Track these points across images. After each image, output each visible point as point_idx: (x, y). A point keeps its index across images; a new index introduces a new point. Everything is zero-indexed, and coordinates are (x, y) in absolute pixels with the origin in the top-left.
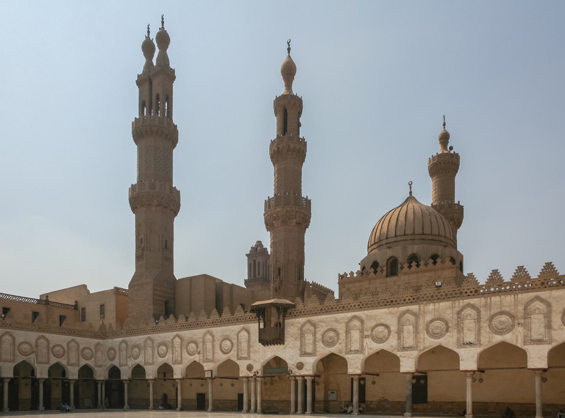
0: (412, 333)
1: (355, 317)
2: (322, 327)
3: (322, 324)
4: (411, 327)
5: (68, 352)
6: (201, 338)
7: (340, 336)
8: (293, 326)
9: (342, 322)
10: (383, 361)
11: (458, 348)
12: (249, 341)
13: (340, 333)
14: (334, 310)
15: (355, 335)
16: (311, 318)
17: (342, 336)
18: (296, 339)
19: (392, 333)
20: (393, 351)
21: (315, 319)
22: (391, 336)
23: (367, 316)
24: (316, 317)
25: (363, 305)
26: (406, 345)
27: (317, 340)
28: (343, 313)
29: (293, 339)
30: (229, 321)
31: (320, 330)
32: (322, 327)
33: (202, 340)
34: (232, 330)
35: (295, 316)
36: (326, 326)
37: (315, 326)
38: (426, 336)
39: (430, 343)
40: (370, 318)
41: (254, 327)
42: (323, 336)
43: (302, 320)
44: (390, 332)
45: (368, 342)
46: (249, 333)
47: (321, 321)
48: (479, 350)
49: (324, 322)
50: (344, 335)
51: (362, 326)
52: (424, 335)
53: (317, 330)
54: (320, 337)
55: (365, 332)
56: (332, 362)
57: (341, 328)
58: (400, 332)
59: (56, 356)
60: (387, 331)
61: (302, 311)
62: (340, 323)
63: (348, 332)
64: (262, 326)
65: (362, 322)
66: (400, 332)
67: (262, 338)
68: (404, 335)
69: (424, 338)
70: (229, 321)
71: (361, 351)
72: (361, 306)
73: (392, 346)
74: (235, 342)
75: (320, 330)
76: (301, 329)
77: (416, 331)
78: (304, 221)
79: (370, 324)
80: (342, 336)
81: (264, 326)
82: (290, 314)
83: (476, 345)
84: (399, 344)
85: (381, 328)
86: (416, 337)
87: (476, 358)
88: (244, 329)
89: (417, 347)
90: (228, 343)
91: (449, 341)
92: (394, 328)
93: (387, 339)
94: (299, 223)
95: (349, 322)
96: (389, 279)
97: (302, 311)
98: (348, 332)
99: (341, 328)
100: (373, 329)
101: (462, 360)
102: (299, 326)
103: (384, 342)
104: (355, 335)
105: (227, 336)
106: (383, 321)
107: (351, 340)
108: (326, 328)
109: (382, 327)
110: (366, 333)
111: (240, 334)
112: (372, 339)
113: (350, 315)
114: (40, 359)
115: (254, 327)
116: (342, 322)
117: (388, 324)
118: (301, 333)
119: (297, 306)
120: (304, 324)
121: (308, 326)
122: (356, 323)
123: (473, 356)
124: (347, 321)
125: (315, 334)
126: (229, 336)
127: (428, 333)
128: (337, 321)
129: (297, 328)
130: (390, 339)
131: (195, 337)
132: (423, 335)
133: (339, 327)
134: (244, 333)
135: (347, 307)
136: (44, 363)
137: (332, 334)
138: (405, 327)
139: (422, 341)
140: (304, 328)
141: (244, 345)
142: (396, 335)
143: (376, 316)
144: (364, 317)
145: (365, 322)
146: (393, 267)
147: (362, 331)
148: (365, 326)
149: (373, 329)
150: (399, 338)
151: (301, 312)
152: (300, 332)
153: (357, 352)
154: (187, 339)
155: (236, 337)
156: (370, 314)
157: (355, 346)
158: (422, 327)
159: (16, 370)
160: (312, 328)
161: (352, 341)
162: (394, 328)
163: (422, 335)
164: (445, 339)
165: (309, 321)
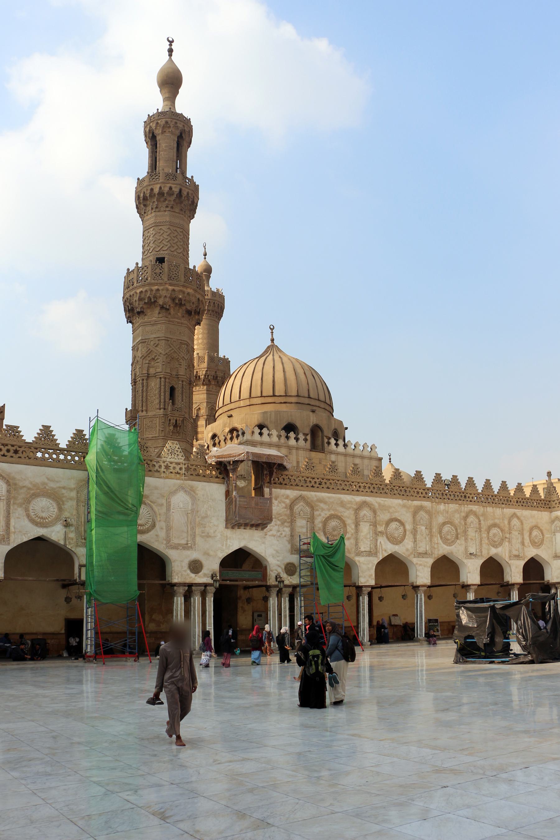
2: (323, 510)
6: (71, 490)
7: (348, 527)
9: (350, 508)
15: (365, 528)
18: (283, 523)
20: (409, 555)
23: (379, 504)
29: (279, 523)
31: (320, 515)
32: (323, 510)
36: (329, 510)
37: (312, 506)
40: (384, 508)
42: (325, 523)
43: (292, 493)
45: (382, 540)
47: (321, 501)
49: (325, 503)
50: (353, 527)
51: (375, 517)
53: (316, 513)
54: (320, 525)
62: (348, 509)
63: (357, 525)
65: (375, 512)
75: (320, 515)
76: (291, 507)
79: (384, 517)
85: (394, 525)
99: (348, 515)
100: (388, 523)
102: (288, 501)
104: (365, 528)
106: (396, 515)
108: (328, 513)
109: (396, 523)
110: (381, 528)
113: (359, 499)
116: (350, 508)
117: (402, 520)
124: (355, 507)
128: (342, 504)
129: (284, 505)
131: (52, 485)
133: (346, 514)
143: (390, 507)
144: (377, 506)
145: (378, 513)
147: (374, 524)
148: (378, 518)
149: (388, 523)
152: (288, 512)
154: (27, 483)
156: (382, 502)
160: (308, 509)
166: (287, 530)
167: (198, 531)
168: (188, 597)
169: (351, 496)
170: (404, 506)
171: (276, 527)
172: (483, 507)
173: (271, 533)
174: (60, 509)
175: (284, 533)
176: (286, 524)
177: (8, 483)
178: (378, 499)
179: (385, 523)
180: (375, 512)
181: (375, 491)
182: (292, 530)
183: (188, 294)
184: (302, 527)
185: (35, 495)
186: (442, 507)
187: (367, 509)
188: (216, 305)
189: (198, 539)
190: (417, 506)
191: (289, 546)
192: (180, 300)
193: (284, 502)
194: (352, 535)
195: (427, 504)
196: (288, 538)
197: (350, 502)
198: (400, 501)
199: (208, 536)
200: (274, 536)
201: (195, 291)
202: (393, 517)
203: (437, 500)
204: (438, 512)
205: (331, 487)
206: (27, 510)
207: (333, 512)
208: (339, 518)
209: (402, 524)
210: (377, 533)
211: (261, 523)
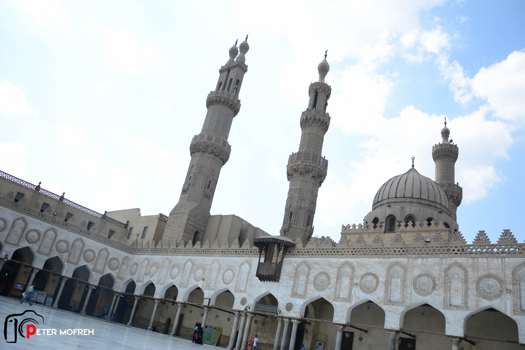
0: (399, 287)
1: (347, 263)
2: (316, 269)
3: (316, 266)
4: (399, 280)
5: (97, 259)
8: (290, 264)
9: (335, 267)
10: (369, 313)
11: (444, 309)
12: (249, 273)
13: (331, 277)
14: (329, 253)
15: (346, 281)
16: (306, 259)
17: (333, 281)
19: (380, 284)
21: (311, 260)
22: (379, 288)
23: (358, 263)
24: (312, 259)
25: (356, 252)
26: (393, 299)
27: (309, 281)
28: (336, 257)
29: (288, 278)
30: (236, 252)
31: (313, 272)
32: (316, 269)
33: (209, 267)
34: (236, 260)
35: (294, 255)
36: (320, 269)
38: (413, 291)
39: (417, 300)
41: (255, 261)
42: (315, 278)
44: (378, 282)
46: (250, 266)
47: (315, 263)
48: (466, 314)
49: (318, 264)
50: (335, 280)
52: (411, 290)
54: (313, 279)
55: (354, 279)
56: (321, 308)
57: (333, 272)
58: (388, 283)
59: (86, 260)
60: (375, 281)
61: (301, 251)
63: (339, 277)
64: (262, 260)
65: (353, 269)
66: (388, 283)
67: (261, 273)
68: (392, 287)
69: (411, 293)
70: (236, 252)
71: (348, 299)
72: (354, 252)
73: (378, 298)
74: (236, 273)
77: (404, 286)
78: (320, 177)
79: (360, 272)
80: (333, 281)
81: (265, 261)
82: (290, 252)
83: (463, 308)
84: (386, 296)
85: (370, 278)
86: (403, 291)
87: (462, 322)
88: (247, 261)
89: (403, 302)
90: (230, 273)
91: (435, 300)
92: (382, 279)
93: (375, 289)
94: (315, 177)
95: (341, 267)
96: (387, 235)
97: (301, 251)
98: (339, 277)
100: (363, 277)
101: (448, 323)
102: (296, 265)
103: (372, 292)
104: (346, 281)
105: (231, 266)
107: (340, 286)
108: (319, 271)
109: (371, 276)
110: (356, 281)
111: (242, 267)
112: (360, 287)
113: (343, 260)
114: (71, 258)
115: (255, 261)
116: (335, 267)
118: (296, 273)
119: (297, 245)
120: (299, 265)
121: (304, 268)
122: (348, 269)
123: (459, 320)
124: (339, 266)
125: (308, 276)
126: (232, 266)
127: (415, 288)
128: (330, 265)
129: (293, 267)
130: (378, 290)
131: (204, 264)
132: (410, 290)
134: (246, 266)
135: (341, 252)
136: (73, 263)
137: (323, 277)
138: (393, 280)
139: (408, 296)
140: (299, 269)
141: (244, 277)
142: (384, 287)
144: (355, 264)
145: (356, 270)
146: (391, 223)
147: (352, 278)
148: (355, 273)
150: (386, 291)
151: (299, 252)
153: (344, 300)
155: (238, 269)
156: (361, 261)
157: (344, 294)
158: (409, 281)
159: (48, 264)
160: (306, 269)
161: (342, 288)
162: (382, 279)
163: (409, 290)
164: (432, 297)
165: (305, 262)
166: (292, 282)
167: (249, 283)
168: (240, 315)
169: (337, 259)
170: (380, 263)
171: (286, 281)
172: (487, 258)
173: (283, 284)
174: (204, 274)
175: (289, 284)
176: (292, 279)
177: (193, 264)
178: (358, 260)
179: (360, 277)
180: (353, 269)
181: (314, 254)
182: (294, 282)
183: (298, 165)
184: (303, 281)
185: (198, 268)
186: (419, 261)
187: (348, 267)
188: (450, 152)
189: (248, 287)
190: (392, 262)
191: (291, 292)
192: (295, 169)
193: (293, 266)
194: (333, 285)
195: (403, 260)
196: (291, 287)
197: (336, 263)
198: (377, 260)
199: (252, 286)
200: (284, 286)
201: (302, 162)
202: (369, 272)
203: (413, 256)
204: (414, 267)
205: (314, 254)
206: (195, 274)
207: (322, 270)
208: (325, 274)
209: (376, 277)
210: (352, 285)
211: (274, 277)
